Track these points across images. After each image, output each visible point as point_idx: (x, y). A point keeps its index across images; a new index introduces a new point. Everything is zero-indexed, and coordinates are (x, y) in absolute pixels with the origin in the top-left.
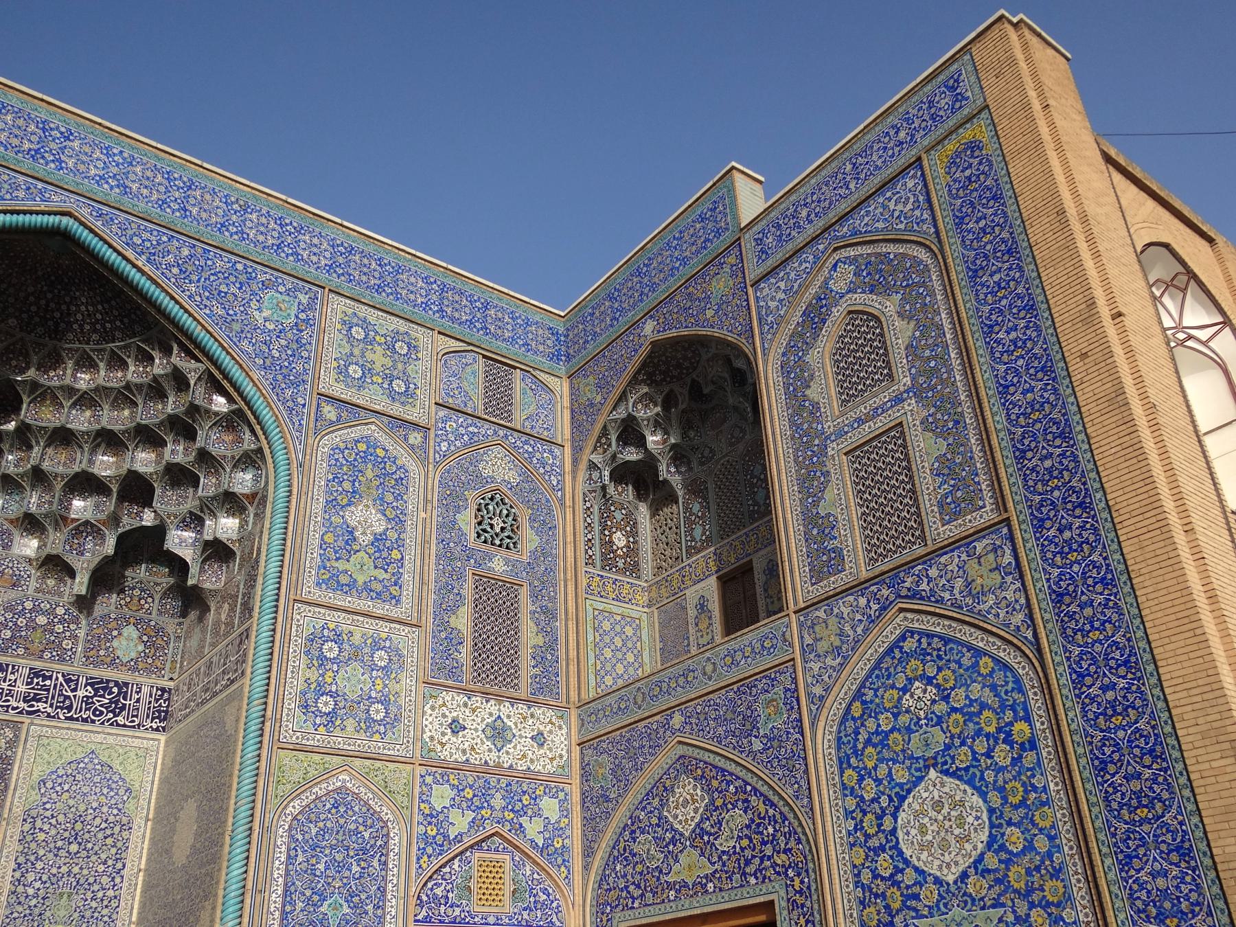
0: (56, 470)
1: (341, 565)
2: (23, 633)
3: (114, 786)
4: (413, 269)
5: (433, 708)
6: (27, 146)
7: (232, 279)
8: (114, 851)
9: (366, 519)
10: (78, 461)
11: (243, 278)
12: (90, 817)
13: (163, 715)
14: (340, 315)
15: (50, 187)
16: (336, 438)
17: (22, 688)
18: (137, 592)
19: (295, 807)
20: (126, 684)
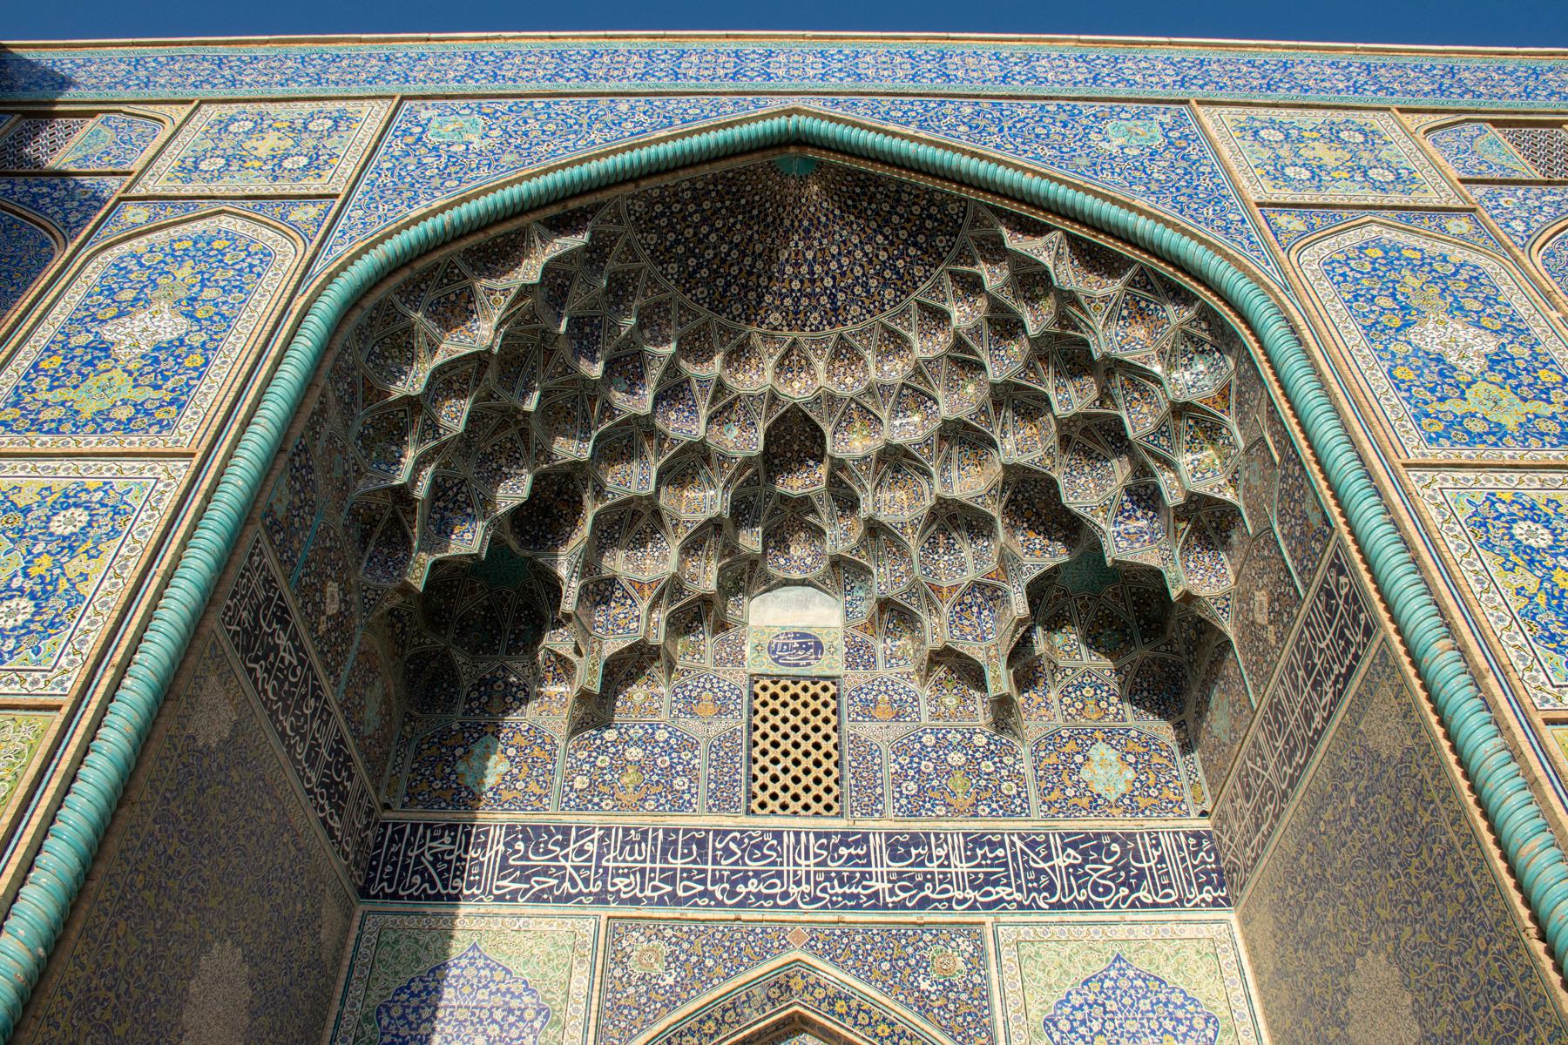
0: (900, 518)
2: (935, 783)
3: (1180, 1014)
10: (927, 493)
16: (1326, 248)
17: (964, 867)
18: (1088, 692)
20: (1130, 836)
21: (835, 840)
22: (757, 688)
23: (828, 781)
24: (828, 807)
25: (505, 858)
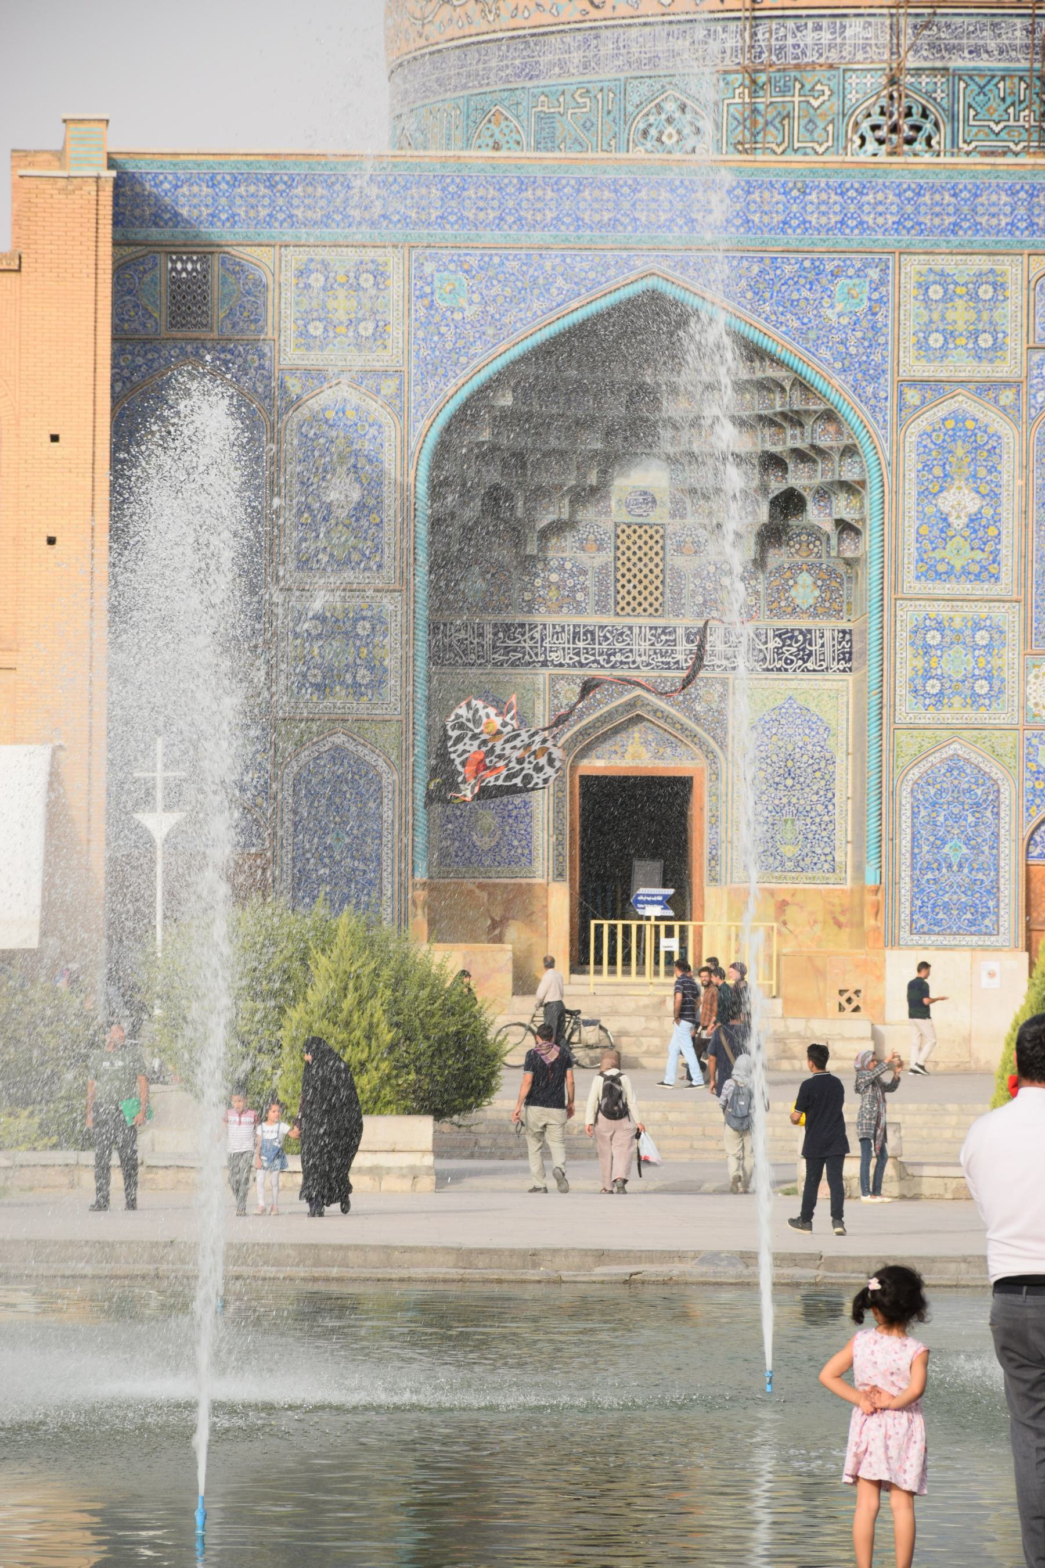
1: (938, 554)
4: (994, 182)
5: (1036, 677)
6: (606, 216)
7: (802, 281)
8: (823, 782)
9: (960, 501)
11: (811, 276)
12: (798, 756)
13: (847, 657)
14: (915, 278)
15: (632, 253)
16: (922, 424)
18: (804, 538)
19: (915, 774)
20: (809, 631)
21: (659, 631)
22: (619, 531)
23: (657, 594)
24: (656, 610)
25: (494, 642)
